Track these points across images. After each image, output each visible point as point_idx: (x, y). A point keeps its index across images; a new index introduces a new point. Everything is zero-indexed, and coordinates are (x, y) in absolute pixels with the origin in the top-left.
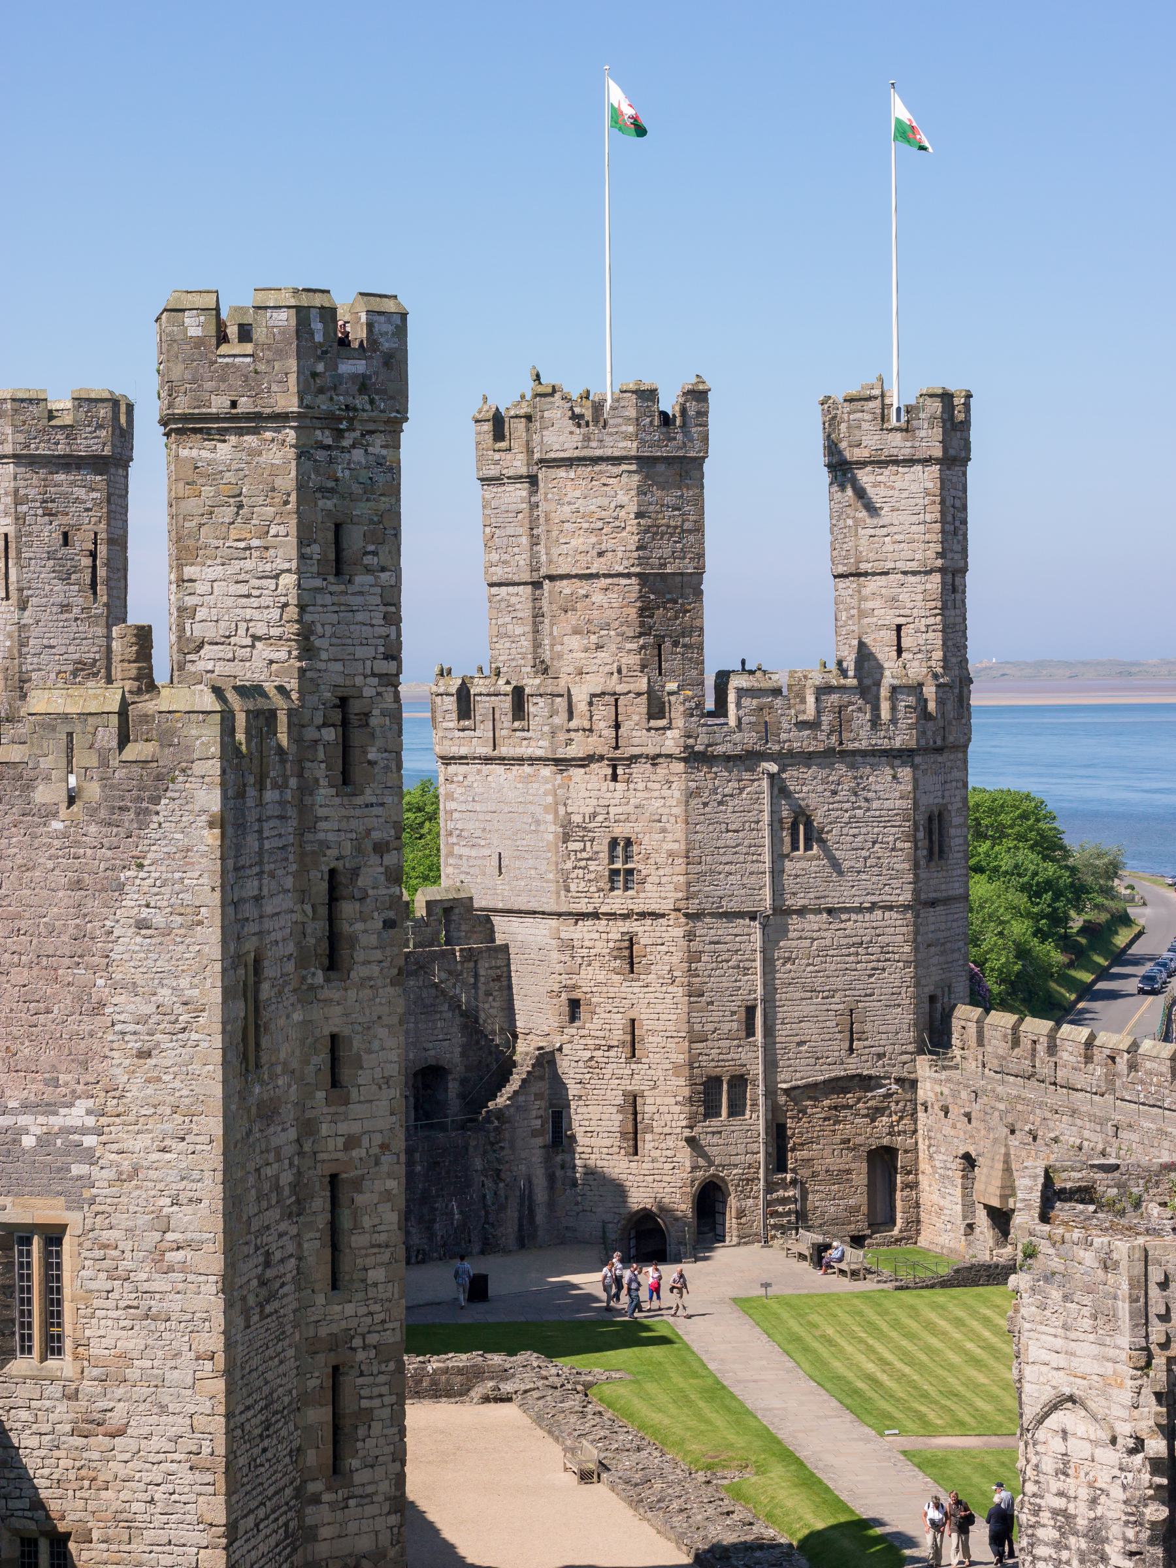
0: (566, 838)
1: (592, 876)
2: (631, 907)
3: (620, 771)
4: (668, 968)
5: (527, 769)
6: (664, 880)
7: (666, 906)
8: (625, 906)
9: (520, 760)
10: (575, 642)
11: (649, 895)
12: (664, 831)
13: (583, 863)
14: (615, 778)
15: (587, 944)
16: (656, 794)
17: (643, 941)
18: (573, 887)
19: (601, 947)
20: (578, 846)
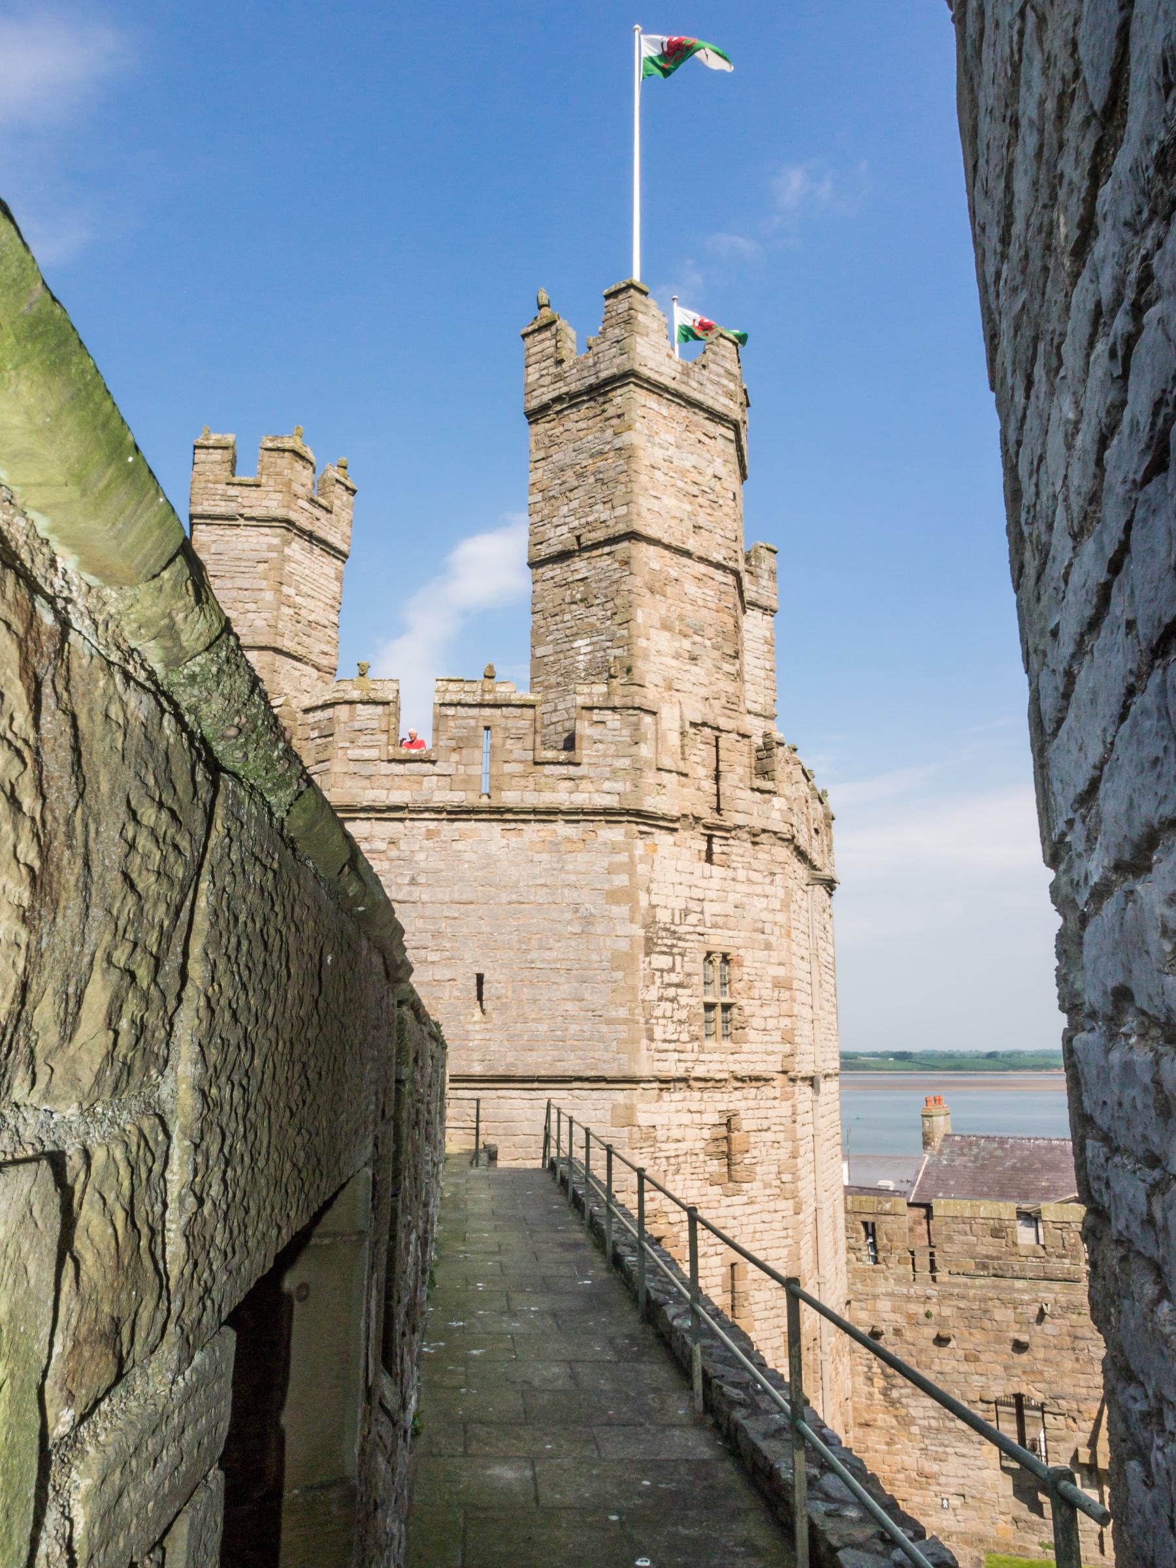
0: (650, 947)
1: (683, 1015)
2: (733, 1067)
3: (716, 848)
4: (775, 1169)
5: (561, 829)
6: (771, 1023)
7: (768, 1066)
8: (725, 1067)
9: (547, 814)
10: (661, 641)
11: (754, 1047)
12: (768, 947)
13: (671, 992)
14: (709, 858)
15: (676, 1133)
16: (758, 889)
17: (746, 1125)
18: (658, 1033)
19: (697, 1139)
20: (663, 961)
